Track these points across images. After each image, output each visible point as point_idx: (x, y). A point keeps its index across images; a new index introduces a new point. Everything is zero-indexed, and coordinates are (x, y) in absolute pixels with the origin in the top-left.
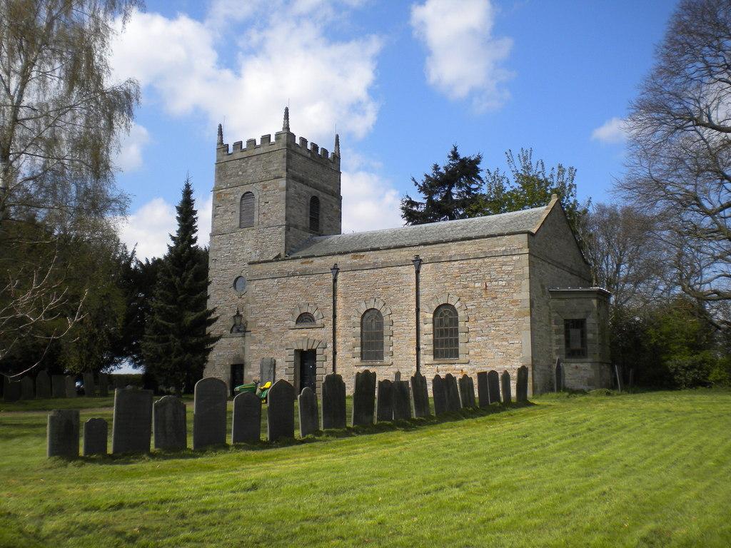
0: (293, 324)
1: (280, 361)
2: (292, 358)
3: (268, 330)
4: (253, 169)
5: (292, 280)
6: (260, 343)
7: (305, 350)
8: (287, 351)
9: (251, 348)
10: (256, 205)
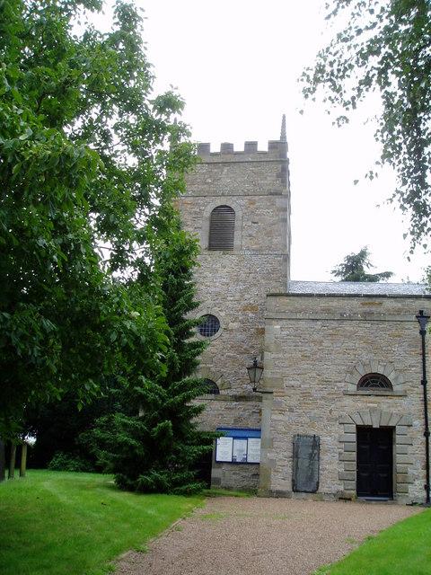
0: (352, 388)
1: (327, 441)
2: (353, 437)
3: (306, 395)
4: (227, 179)
5: (348, 326)
6: (291, 410)
7: (376, 426)
8: (342, 426)
9: (274, 417)
10: (237, 224)
